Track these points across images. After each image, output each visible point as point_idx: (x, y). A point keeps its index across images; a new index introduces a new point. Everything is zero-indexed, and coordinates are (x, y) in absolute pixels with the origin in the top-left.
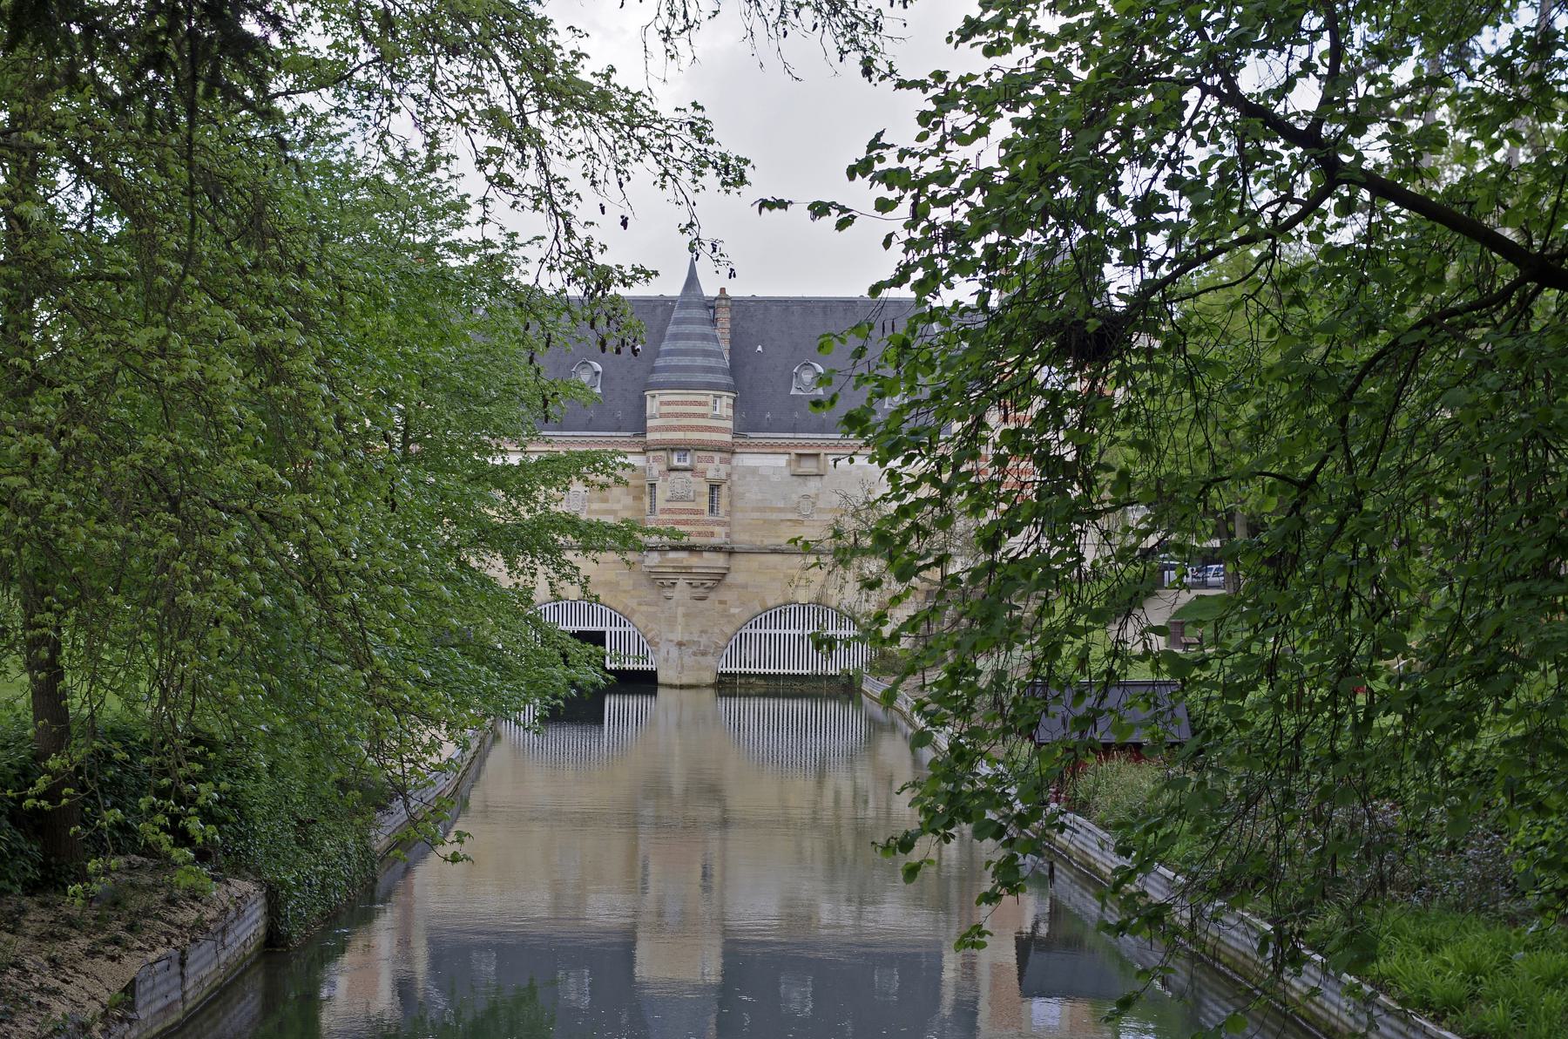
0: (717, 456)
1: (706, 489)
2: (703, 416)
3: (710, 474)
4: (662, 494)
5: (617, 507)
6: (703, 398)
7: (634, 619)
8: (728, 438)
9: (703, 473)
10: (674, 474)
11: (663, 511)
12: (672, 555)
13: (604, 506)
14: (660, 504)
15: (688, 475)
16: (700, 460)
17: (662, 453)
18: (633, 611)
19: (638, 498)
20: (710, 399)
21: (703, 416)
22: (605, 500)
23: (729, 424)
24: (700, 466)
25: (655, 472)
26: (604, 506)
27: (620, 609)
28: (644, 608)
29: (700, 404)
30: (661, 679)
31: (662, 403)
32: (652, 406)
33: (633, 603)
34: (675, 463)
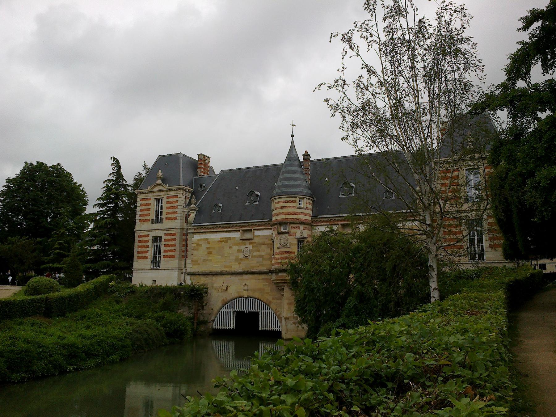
0: (301, 227)
1: (296, 242)
2: (294, 207)
3: (298, 235)
4: (276, 245)
5: (263, 253)
6: (293, 199)
7: (271, 306)
8: (309, 218)
9: (294, 234)
10: (281, 236)
11: (277, 253)
12: (280, 274)
13: (258, 253)
14: (276, 250)
15: (287, 235)
16: (292, 228)
17: (276, 226)
18: (270, 302)
19: (271, 249)
20: (298, 199)
21: (294, 207)
22: (258, 251)
23: (310, 212)
24: (293, 231)
25: (274, 236)
26: (258, 253)
27: (265, 301)
28: (275, 301)
29: (292, 202)
30: (284, 335)
31: (276, 203)
32: (274, 205)
33: (270, 298)
34: (282, 230)
